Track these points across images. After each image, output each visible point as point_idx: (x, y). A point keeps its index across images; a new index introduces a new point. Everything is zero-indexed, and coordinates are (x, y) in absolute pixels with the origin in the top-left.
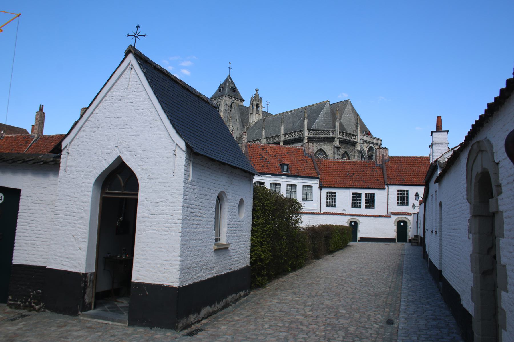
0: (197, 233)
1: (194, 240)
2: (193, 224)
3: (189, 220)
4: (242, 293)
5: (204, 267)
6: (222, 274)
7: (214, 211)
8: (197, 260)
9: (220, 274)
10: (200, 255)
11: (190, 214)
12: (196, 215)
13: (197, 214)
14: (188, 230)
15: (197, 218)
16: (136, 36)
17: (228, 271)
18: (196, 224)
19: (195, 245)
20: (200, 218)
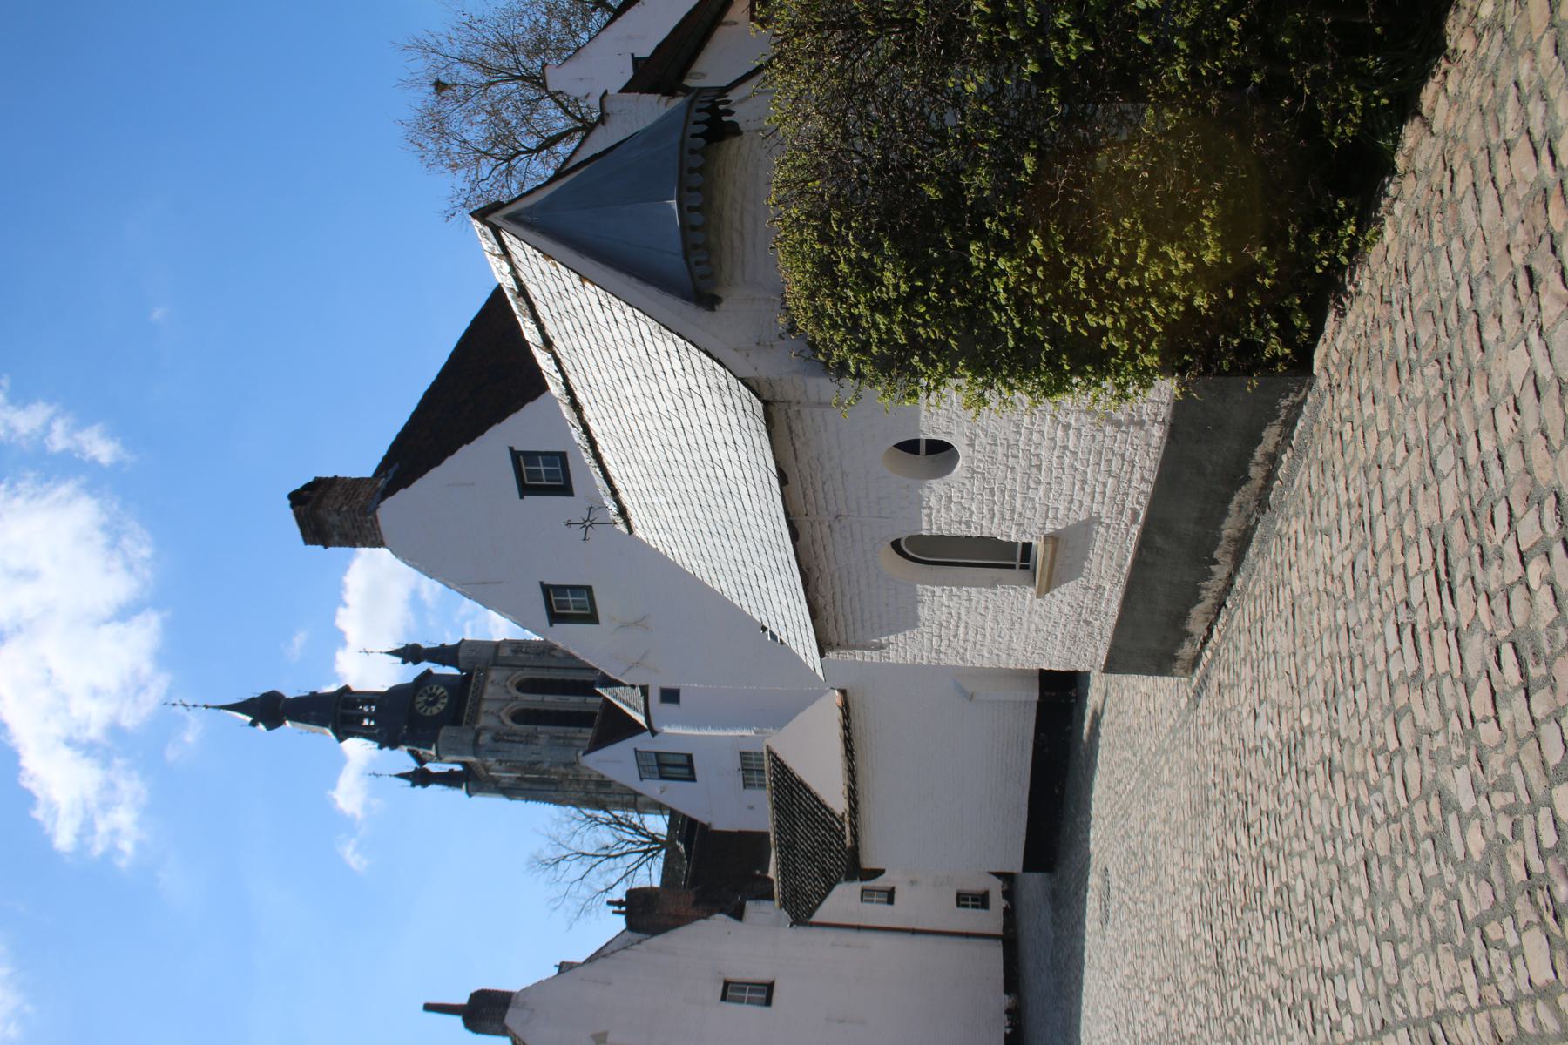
0: (997, 634)
1: (1011, 640)
2: (975, 643)
3: (966, 650)
4: (1271, 435)
5: (1085, 615)
6: (1130, 557)
7: (943, 590)
8: (1059, 635)
9: (1126, 569)
10: (1050, 627)
11: (954, 649)
12: (956, 636)
13: (952, 633)
14: (986, 654)
15: (961, 631)
16: (588, 523)
17: (1135, 530)
18: (976, 635)
19: (1024, 639)
20: (962, 625)
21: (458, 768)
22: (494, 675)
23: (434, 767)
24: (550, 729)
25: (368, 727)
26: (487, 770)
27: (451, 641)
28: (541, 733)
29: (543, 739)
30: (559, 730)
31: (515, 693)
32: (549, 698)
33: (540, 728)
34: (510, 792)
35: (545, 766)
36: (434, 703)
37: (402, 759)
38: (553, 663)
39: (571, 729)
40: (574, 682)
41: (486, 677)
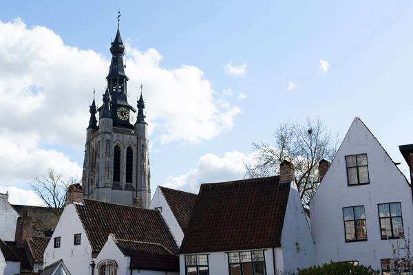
21: (98, 125)
22: (134, 138)
23: (97, 115)
24: (113, 161)
25: (113, 89)
26: (96, 136)
27: (146, 120)
28: (111, 159)
29: (108, 159)
30: (112, 165)
31: (128, 146)
32: (125, 160)
33: (113, 157)
34: (88, 144)
35: (98, 160)
36: (122, 115)
37: (99, 104)
38: (139, 161)
39: (113, 170)
40: (131, 169)
41: (133, 135)
